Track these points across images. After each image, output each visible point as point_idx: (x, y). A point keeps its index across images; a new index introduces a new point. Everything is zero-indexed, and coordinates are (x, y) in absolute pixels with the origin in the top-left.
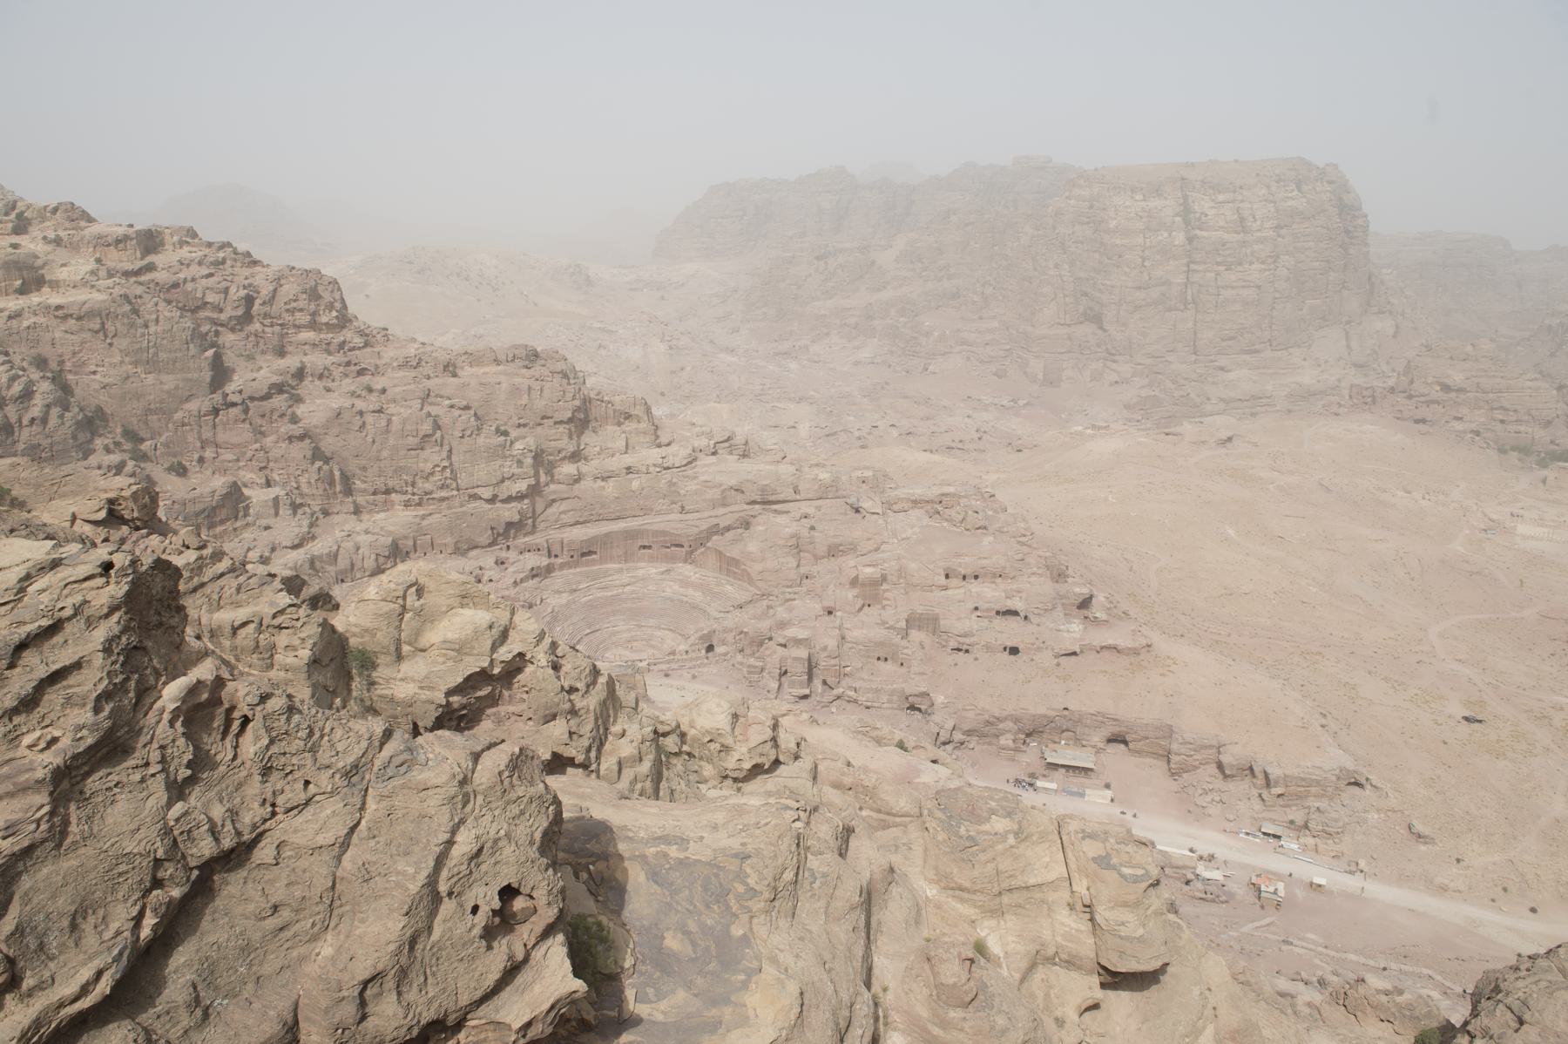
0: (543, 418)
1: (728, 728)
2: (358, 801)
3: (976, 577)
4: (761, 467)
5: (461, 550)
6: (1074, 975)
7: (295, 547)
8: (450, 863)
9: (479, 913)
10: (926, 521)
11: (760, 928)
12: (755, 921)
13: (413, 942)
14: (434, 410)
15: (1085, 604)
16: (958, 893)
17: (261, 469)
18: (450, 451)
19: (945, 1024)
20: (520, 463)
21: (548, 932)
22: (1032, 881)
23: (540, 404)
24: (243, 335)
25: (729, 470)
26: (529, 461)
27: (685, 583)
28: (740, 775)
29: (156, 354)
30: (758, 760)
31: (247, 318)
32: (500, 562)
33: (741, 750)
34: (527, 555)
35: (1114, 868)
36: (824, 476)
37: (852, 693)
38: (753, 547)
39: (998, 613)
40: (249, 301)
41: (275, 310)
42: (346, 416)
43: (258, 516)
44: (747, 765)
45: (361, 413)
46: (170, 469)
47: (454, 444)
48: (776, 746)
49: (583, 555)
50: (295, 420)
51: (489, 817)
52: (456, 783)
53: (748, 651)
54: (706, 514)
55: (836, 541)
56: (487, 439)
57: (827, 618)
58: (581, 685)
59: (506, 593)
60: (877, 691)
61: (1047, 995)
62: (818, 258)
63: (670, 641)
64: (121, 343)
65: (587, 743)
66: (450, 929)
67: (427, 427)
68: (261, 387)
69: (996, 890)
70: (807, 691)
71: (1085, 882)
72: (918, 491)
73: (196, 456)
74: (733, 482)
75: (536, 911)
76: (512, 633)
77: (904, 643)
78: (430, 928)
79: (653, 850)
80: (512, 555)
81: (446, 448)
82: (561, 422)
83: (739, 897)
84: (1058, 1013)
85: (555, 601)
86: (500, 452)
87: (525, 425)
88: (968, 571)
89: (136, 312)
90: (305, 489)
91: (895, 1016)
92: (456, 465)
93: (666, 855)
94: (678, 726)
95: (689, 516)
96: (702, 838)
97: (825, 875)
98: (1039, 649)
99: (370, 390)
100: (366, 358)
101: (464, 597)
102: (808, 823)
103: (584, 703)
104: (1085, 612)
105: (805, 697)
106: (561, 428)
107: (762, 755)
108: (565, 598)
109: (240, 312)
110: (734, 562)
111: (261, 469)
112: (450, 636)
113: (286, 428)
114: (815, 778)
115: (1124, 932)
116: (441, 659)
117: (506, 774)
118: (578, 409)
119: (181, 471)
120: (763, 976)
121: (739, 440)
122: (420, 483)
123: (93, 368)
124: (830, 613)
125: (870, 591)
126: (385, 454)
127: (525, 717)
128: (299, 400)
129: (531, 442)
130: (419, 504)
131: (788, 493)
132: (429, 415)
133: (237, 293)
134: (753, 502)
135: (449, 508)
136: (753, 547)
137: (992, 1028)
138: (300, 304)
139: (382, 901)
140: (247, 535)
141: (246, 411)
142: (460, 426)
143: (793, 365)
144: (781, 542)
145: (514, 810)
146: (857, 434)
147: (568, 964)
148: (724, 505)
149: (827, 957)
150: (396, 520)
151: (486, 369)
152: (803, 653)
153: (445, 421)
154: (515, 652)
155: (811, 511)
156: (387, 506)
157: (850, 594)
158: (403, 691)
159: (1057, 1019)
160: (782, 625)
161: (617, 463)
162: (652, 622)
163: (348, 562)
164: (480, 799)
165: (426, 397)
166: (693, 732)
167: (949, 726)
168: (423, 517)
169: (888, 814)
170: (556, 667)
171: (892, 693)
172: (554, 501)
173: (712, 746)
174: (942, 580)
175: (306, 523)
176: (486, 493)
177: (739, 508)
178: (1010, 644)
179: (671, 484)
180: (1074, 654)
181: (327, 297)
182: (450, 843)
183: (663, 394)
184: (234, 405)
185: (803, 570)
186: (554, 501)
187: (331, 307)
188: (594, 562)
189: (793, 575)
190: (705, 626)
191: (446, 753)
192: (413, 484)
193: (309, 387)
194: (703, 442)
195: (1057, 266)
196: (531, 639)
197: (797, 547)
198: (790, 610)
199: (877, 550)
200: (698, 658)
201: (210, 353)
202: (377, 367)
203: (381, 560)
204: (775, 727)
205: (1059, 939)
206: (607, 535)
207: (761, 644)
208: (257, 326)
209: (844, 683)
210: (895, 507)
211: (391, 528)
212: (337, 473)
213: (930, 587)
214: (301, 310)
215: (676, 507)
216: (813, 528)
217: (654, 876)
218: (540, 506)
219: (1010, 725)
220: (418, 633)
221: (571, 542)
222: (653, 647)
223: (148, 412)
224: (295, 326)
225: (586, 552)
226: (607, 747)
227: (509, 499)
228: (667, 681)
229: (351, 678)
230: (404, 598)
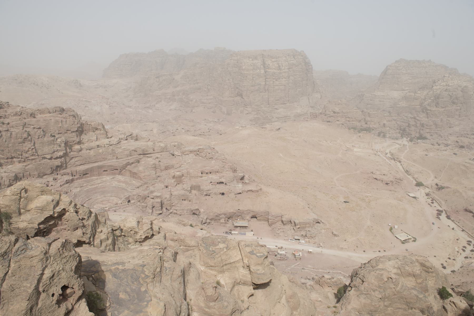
1: (136, 226)
2: (7, 264)
3: (210, 173)
4: (142, 143)
5: (40, 176)
6: (246, 287)
8: (43, 281)
9: (55, 296)
10: (194, 157)
11: (150, 287)
12: (149, 285)
13: (31, 309)
15: (242, 178)
16: (211, 268)
18: (34, 143)
19: (209, 307)
20: (60, 146)
21: (80, 299)
22: (232, 261)
23: (66, 126)
25: (132, 145)
26: (63, 145)
27: (119, 181)
28: (142, 240)
30: (147, 235)
32: (55, 179)
33: (141, 232)
34: (64, 176)
35: (255, 254)
36: (162, 145)
38: (141, 168)
44: (143, 237)
47: (36, 141)
48: (152, 230)
49: (84, 175)
51: (56, 264)
52: (43, 254)
53: (141, 201)
54: (125, 159)
56: (47, 138)
58: (86, 217)
59: (58, 189)
60: (183, 210)
61: (238, 294)
63: (115, 200)
65: (89, 236)
66: (45, 303)
67: (25, 135)
69: (222, 265)
70: (161, 212)
71: (247, 260)
72: (192, 148)
74: (133, 148)
75: (74, 292)
76: (60, 202)
77: (190, 194)
78: (37, 304)
79: (113, 268)
80: (59, 176)
81: (33, 142)
82: (74, 132)
83: (143, 279)
84: (242, 299)
85: (75, 191)
86: (52, 143)
87: (61, 133)
88: (208, 171)
91: (194, 308)
92: (37, 148)
93: (118, 269)
94: (120, 227)
96: (129, 262)
97: (170, 268)
98: (230, 193)
99: (3, 124)
101: (42, 192)
102: (163, 253)
103: (87, 223)
104: (243, 181)
105: (161, 214)
106: (74, 134)
107: (148, 233)
108: (79, 189)
110: (135, 173)
112: (38, 205)
114: (165, 238)
115: (259, 272)
116: (35, 213)
117: (61, 249)
118: (79, 127)
120: (152, 302)
121: (134, 135)
122: (24, 155)
124: (167, 187)
125: (179, 180)
126: (10, 145)
127: (67, 229)
129: (63, 138)
130: (24, 162)
131: (151, 151)
132: (26, 131)
134: (140, 154)
135: (35, 162)
136: (141, 168)
137: (223, 306)
139: (19, 297)
142: (37, 134)
143: (150, 111)
144: (150, 166)
145: (65, 260)
146: (172, 131)
147: (87, 308)
148: (131, 156)
149: (172, 293)
150: (16, 167)
152: (159, 200)
153: (32, 133)
154: (62, 208)
155: (159, 156)
156: (12, 163)
157: (173, 181)
158: (22, 225)
159: (242, 301)
160: (152, 192)
161: (94, 144)
162: (109, 195)
164: (52, 258)
165: (24, 125)
166: (125, 228)
167: (205, 218)
168: (26, 166)
170: (77, 212)
172: (73, 158)
173: (132, 232)
174: (200, 175)
176: (49, 157)
177: (136, 157)
178: (221, 192)
179: (113, 150)
180: (240, 193)
182: (42, 274)
183: (108, 121)
185: (157, 175)
186: (73, 158)
188: (88, 177)
189: (154, 176)
190: (127, 195)
191: (39, 244)
192: (22, 155)
194: (122, 136)
195: (229, 80)
196: (67, 203)
197: (155, 167)
198: (154, 187)
199: (180, 167)
200: (125, 205)
202: (5, 115)
203: (11, 181)
204: (152, 224)
205: (241, 277)
206: (92, 168)
207: (145, 198)
209: (172, 208)
210: (185, 153)
211: (14, 170)
213: (197, 177)
215: (115, 157)
216: (160, 161)
217: (115, 276)
218: (68, 159)
220: (26, 205)
221: (80, 171)
222: (110, 202)
225: (85, 174)
226: (96, 236)
227: (57, 158)
228: (115, 213)
229: (2, 223)
230: (20, 193)
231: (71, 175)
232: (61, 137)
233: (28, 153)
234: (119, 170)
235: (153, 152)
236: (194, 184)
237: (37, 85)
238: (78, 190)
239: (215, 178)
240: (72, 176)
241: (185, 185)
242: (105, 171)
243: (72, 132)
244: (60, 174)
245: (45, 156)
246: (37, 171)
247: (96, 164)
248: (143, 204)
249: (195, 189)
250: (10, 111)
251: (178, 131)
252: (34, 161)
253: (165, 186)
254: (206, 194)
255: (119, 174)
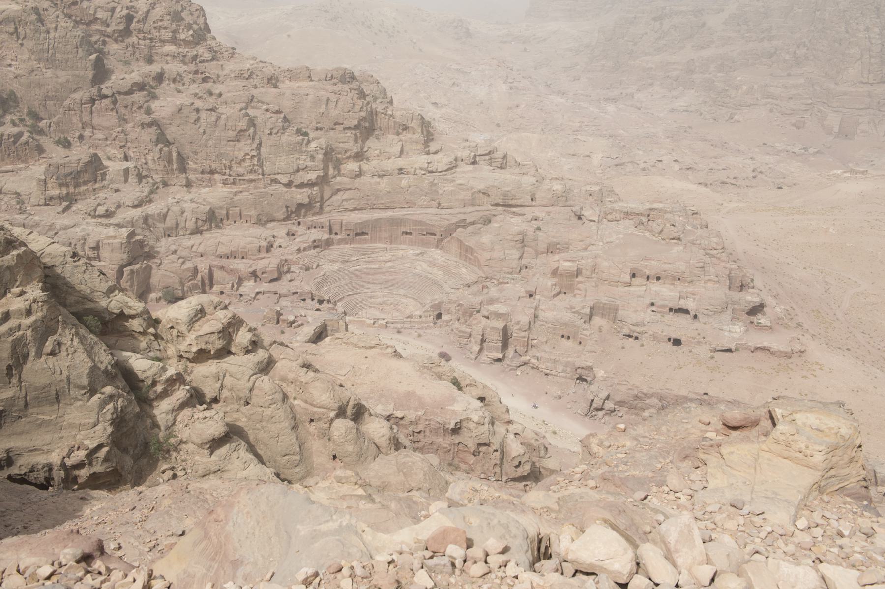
0: (336, 124)
3: (658, 278)
4: (508, 176)
5: (262, 221)
7: (135, 207)
10: (632, 229)
14: (251, 112)
15: (756, 310)
17: (121, 147)
18: (260, 144)
20: (313, 158)
23: (334, 113)
24: (124, 45)
25: (486, 176)
26: (320, 157)
27: (433, 264)
28: (191, 356)
29: (54, 54)
31: (126, 32)
32: (291, 234)
34: (313, 230)
36: (557, 187)
37: (534, 361)
39: (671, 310)
40: (129, 19)
41: (147, 27)
42: (186, 111)
43: (112, 181)
45: (198, 110)
46: (58, 142)
47: (264, 139)
49: (357, 234)
50: (149, 112)
53: (462, 320)
54: (458, 210)
55: (555, 240)
57: (528, 300)
59: (290, 257)
60: (555, 361)
62: (655, 19)
64: (29, 44)
67: (243, 124)
68: (126, 85)
70: (500, 356)
72: (632, 206)
73: (77, 134)
74: (481, 187)
77: (586, 326)
80: (301, 229)
81: (257, 141)
82: (349, 128)
85: (328, 268)
86: (297, 148)
87: (321, 129)
89: (41, 21)
90: (151, 165)
92: (263, 155)
95: (444, 211)
98: (699, 343)
99: (211, 94)
100: (212, 69)
104: (752, 318)
105: (499, 360)
106: (349, 133)
108: (337, 266)
109: (121, 27)
110: (470, 250)
111: (121, 147)
113: (141, 117)
118: (364, 119)
119: (67, 144)
121: (499, 155)
123: (9, 62)
124: (531, 296)
125: (567, 281)
126: (211, 143)
128: (155, 97)
129: (323, 142)
130: (234, 183)
131: (527, 200)
132: (247, 115)
133: (121, 12)
134: (497, 205)
135: (255, 188)
136: (486, 239)
138: (165, 23)
140: (102, 195)
141: (115, 102)
142: (269, 125)
143: (611, 108)
144: (509, 237)
146: (642, 165)
148: (473, 205)
150: (215, 194)
151: (300, 84)
152: (500, 325)
153: (259, 121)
156: (211, 183)
157: (550, 282)
160: (491, 302)
162: (402, 292)
163: (174, 221)
167: (603, 395)
168: (236, 194)
169: (312, 404)
171: (567, 365)
172: (339, 190)
174: (627, 278)
175: (147, 190)
176: (284, 179)
177: (485, 208)
178: (674, 336)
179: (432, 184)
180: (730, 350)
181: (189, 19)
183: (498, 125)
184: (106, 97)
185: (524, 261)
186: (339, 190)
187: (189, 27)
188: (366, 242)
190: (438, 297)
192: (230, 168)
193: (167, 87)
194: (465, 154)
195: (867, 29)
197: (522, 242)
199: (586, 249)
200: (426, 322)
201: (94, 56)
202: (218, 76)
203: (200, 223)
207: (471, 315)
208: (134, 39)
209: (530, 353)
210: (609, 217)
211: (211, 200)
212: (174, 155)
214: (165, 28)
215: (435, 203)
216: (539, 229)
218: (327, 194)
219: (655, 401)
222: (398, 310)
223: (47, 98)
224: (161, 41)
225: (360, 233)
227: (302, 186)
231: (327, 229)
232: (318, 138)
233: (244, 164)
234: (439, 236)
235: (530, 203)
236: (604, 300)
237: (369, 27)
238: (335, 268)
239: (667, 293)
240: (331, 232)
241: (579, 299)
242: (407, 233)
243: (345, 129)
244: (305, 223)
245: (276, 176)
246: (255, 208)
247: (389, 214)
248: (463, 328)
249: (603, 315)
250: (231, 67)
251: (660, 165)
252: (252, 185)
253: (527, 292)
254: (628, 332)
255: (437, 247)
